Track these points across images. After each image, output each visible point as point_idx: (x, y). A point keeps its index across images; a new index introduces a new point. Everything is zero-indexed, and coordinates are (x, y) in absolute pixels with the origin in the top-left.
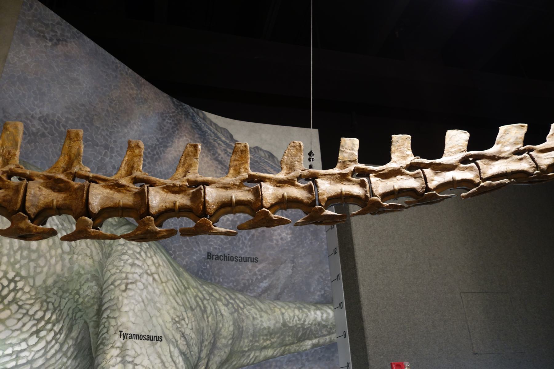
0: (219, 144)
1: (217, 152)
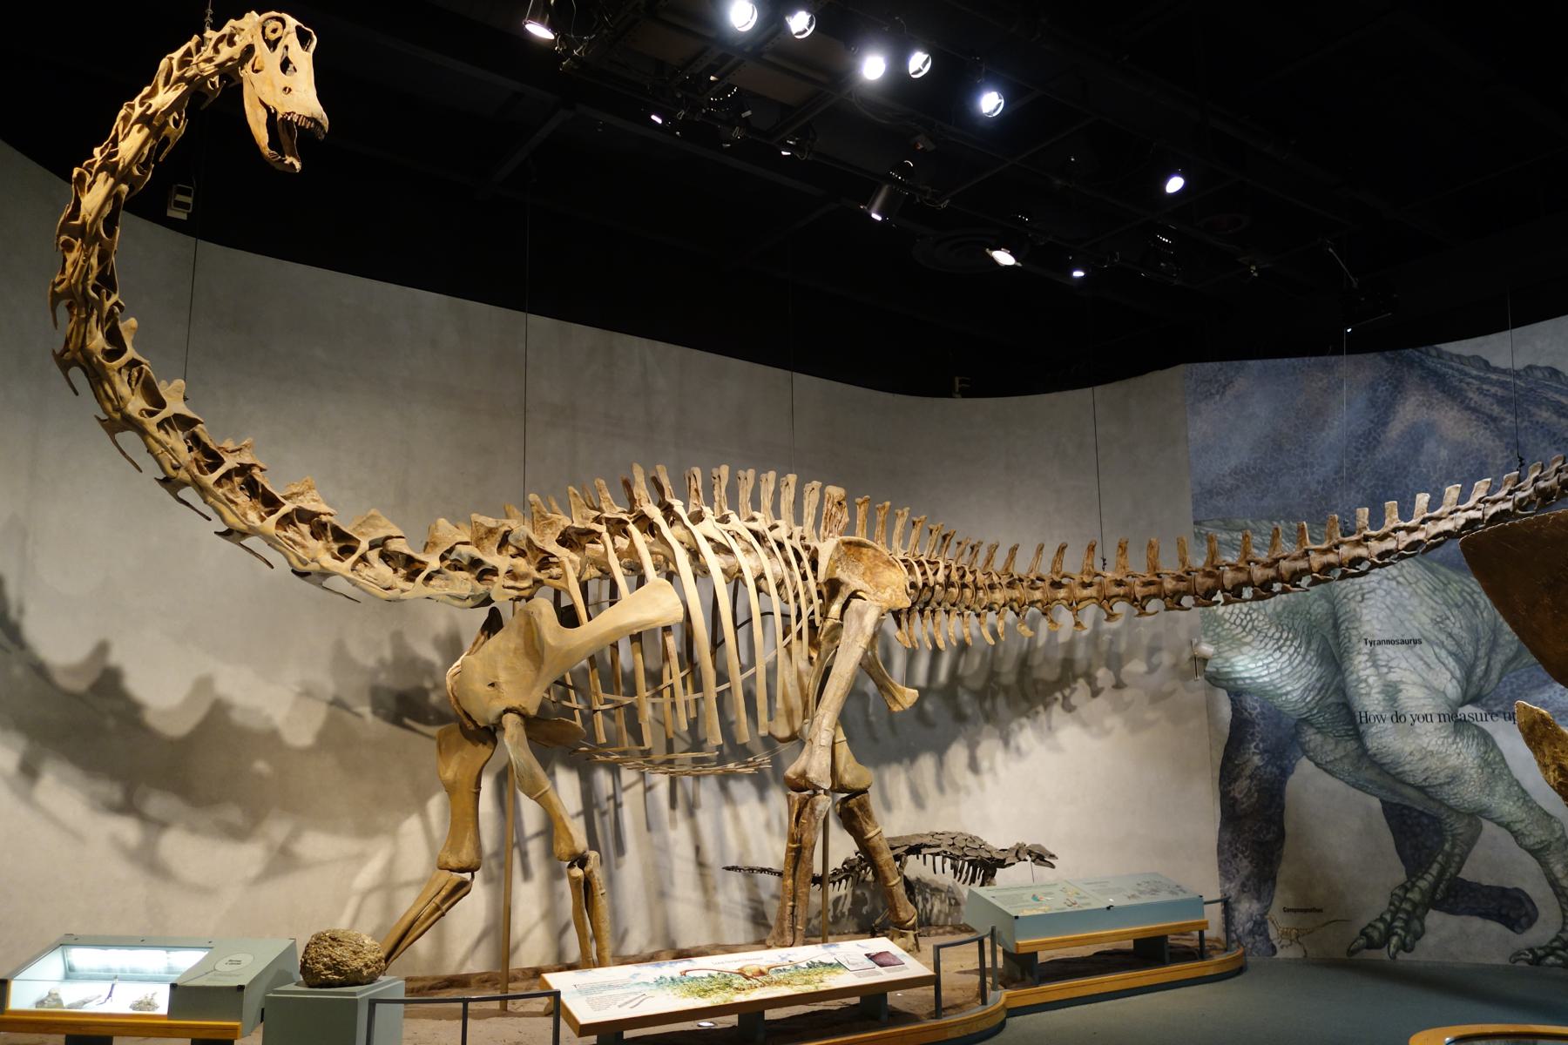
0: (1468, 384)
1: (1466, 397)
